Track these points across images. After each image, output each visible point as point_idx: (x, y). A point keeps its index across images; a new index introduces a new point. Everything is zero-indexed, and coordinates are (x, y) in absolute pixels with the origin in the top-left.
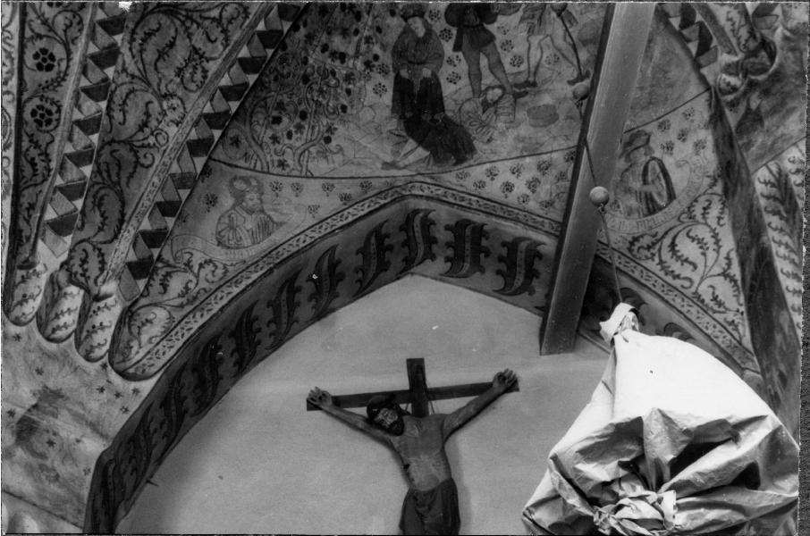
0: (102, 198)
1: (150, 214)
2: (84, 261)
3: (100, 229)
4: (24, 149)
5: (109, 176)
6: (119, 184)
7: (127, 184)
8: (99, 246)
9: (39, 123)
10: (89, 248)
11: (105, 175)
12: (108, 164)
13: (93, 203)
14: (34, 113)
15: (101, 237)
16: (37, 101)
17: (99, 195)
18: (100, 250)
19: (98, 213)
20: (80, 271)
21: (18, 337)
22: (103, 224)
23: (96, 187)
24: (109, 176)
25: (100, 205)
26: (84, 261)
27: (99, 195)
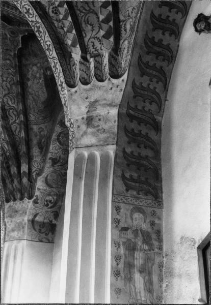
0: (88, 19)
1: (101, 12)
2: (93, 46)
3: (92, 31)
4: (57, 26)
5: (86, 10)
6: (91, 9)
7: (94, 6)
8: (96, 36)
9: (56, 13)
10: (92, 40)
11: (84, 11)
12: (82, 7)
13: (85, 24)
14: (53, 12)
15: (94, 33)
16: (51, 7)
17: (86, 20)
18: (97, 37)
19: (89, 26)
20: (94, 50)
21: (76, 91)
22: (92, 28)
23: (83, 18)
24: (86, 10)
25: (88, 23)
26: (93, 46)
27: (86, 20)
